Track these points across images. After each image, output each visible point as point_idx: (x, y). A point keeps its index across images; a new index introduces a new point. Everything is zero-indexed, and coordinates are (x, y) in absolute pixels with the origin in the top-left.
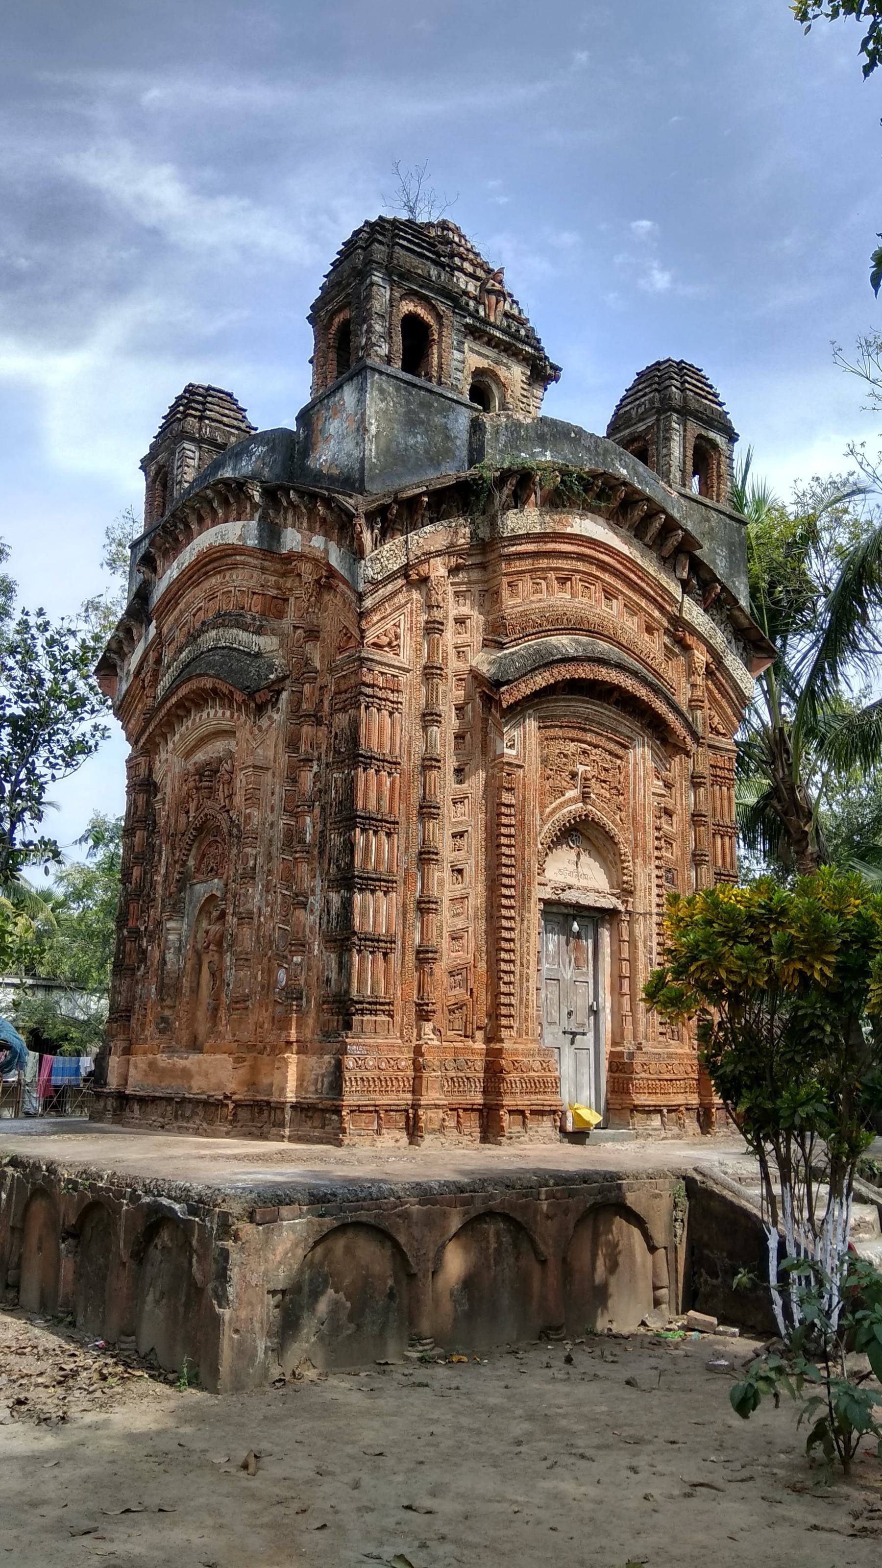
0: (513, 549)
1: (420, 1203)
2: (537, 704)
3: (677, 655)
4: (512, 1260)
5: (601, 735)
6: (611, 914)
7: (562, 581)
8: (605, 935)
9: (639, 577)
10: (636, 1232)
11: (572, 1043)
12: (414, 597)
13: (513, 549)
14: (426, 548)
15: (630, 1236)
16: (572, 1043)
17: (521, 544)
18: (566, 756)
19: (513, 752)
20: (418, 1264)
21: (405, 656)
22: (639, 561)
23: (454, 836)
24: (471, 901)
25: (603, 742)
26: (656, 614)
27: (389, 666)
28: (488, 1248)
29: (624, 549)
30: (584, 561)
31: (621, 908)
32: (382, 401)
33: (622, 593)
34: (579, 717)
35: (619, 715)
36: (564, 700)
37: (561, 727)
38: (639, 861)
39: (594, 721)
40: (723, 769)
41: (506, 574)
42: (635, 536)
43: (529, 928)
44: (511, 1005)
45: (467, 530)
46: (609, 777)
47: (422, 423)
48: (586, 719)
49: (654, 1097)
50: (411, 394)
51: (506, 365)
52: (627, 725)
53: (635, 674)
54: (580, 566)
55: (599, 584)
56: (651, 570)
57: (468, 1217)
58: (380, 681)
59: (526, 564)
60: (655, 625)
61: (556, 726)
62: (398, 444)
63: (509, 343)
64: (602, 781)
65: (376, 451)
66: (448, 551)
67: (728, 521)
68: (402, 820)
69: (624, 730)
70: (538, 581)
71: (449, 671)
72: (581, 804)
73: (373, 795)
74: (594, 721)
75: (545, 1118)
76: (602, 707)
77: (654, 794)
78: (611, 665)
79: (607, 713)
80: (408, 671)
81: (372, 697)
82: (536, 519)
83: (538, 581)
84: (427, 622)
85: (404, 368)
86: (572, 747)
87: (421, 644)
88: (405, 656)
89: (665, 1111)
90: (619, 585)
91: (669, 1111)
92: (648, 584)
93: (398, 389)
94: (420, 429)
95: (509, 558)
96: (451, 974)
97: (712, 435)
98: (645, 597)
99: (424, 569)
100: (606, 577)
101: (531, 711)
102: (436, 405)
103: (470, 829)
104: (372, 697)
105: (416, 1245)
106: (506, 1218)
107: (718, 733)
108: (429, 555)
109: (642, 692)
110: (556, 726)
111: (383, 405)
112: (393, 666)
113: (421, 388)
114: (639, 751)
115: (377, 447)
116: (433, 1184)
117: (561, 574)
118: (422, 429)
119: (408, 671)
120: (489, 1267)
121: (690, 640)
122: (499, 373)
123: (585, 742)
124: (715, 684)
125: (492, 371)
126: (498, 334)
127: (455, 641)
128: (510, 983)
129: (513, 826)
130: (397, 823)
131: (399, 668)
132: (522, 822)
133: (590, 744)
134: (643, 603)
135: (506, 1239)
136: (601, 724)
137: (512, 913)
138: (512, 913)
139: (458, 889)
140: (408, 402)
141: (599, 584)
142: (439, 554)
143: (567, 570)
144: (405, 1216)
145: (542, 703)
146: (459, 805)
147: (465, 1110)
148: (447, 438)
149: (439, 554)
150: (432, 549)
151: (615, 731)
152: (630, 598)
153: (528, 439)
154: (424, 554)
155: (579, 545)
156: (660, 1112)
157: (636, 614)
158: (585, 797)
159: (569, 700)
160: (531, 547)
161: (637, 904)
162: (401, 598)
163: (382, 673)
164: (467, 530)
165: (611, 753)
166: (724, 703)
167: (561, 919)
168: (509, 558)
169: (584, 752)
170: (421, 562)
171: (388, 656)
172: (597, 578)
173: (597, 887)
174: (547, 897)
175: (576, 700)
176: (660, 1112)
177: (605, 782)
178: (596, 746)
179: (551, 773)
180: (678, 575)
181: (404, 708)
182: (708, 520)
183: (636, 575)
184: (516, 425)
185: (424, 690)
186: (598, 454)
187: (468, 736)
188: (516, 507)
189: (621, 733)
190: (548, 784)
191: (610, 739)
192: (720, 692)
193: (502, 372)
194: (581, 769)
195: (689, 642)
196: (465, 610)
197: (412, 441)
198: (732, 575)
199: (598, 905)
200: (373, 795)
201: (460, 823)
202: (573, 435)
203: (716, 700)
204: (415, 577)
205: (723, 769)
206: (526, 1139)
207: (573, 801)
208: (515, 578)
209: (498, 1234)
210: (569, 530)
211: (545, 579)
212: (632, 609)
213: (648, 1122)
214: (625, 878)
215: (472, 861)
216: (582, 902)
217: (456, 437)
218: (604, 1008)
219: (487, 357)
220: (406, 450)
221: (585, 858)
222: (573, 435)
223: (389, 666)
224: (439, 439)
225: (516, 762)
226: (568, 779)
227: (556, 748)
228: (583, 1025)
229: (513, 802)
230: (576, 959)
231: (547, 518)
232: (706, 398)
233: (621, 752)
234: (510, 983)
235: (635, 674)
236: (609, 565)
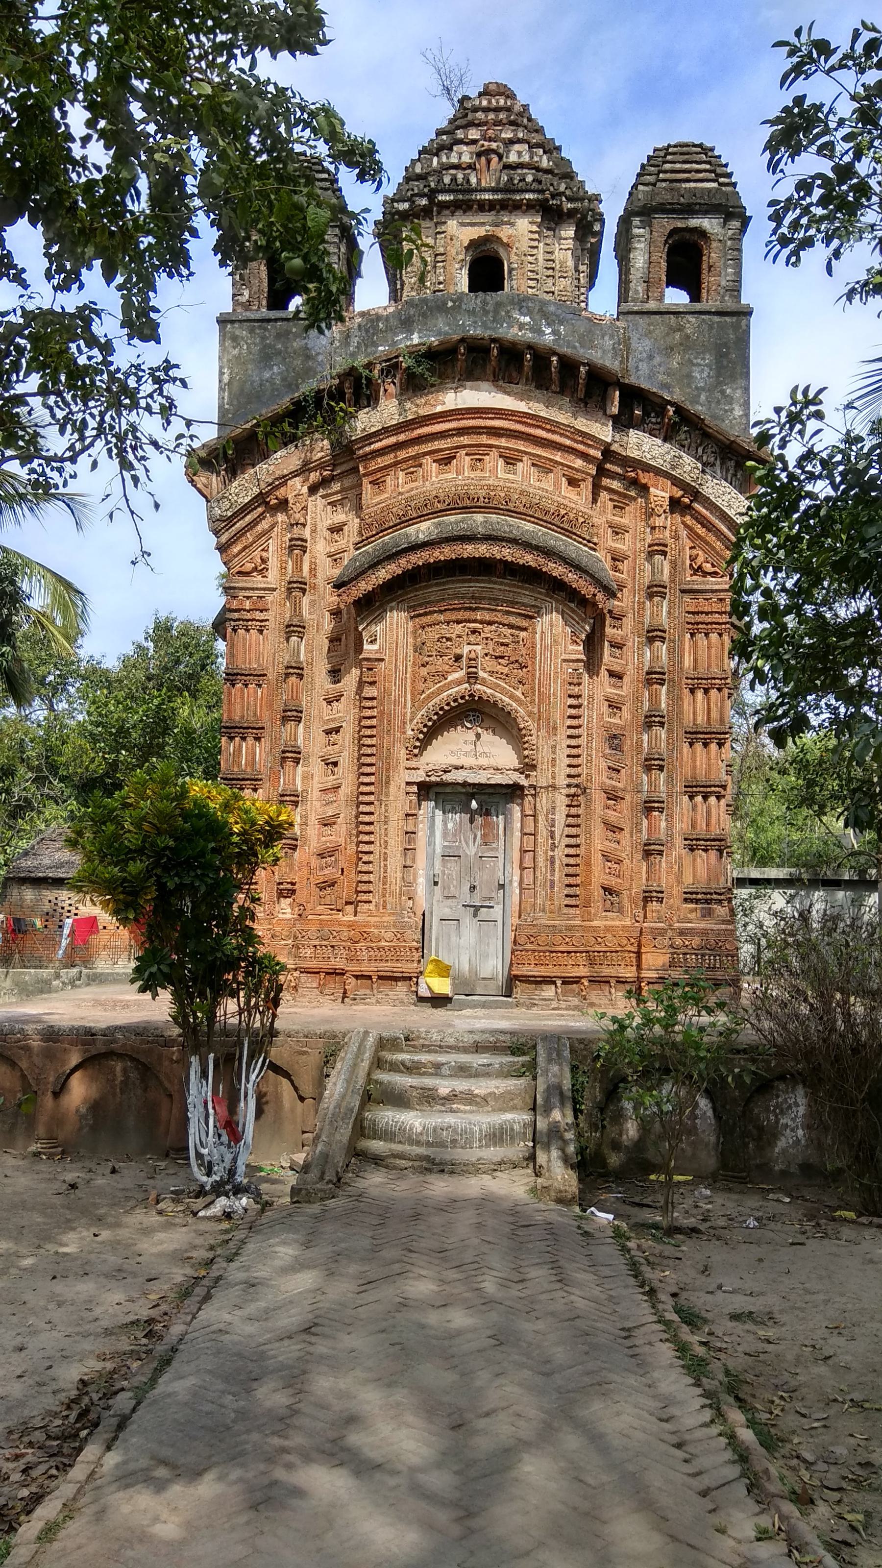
0: (367, 449)
1: (41, 1040)
2: (401, 596)
3: (635, 499)
4: (139, 1092)
5: (495, 610)
6: (513, 792)
7: (446, 461)
8: (516, 809)
9: (548, 431)
10: (285, 1082)
11: (475, 915)
12: (280, 519)
13: (367, 449)
14: (278, 473)
15: (277, 1085)
16: (475, 915)
17: (381, 440)
18: (448, 639)
19: (375, 647)
20: (37, 1085)
21: (273, 577)
22: (542, 414)
23: (328, 732)
24: (343, 791)
25: (499, 617)
26: (579, 463)
27: (253, 589)
28: (114, 1080)
29: (521, 406)
30: (468, 434)
31: (524, 782)
32: (234, 348)
33: (527, 453)
34: (463, 598)
35: (514, 586)
36: (437, 585)
37: (441, 612)
38: (543, 733)
39: (484, 598)
40: (712, 613)
41: (365, 475)
42: (537, 387)
43: (386, 811)
44: (370, 882)
45: (326, 442)
46: (507, 651)
47: (279, 353)
48: (473, 597)
49: (542, 968)
50: (266, 329)
51: (507, 223)
52: (526, 595)
53: (514, 541)
54: (465, 440)
55: (494, 453)
56: (562, 417)
57: (88, 1055)
58: (247, 605)
59: (388, 459)
60: (578, 476)
61: (435, 612)
62: (253, 382)
63: (503, 200)
64: (496, 658)
65: (229, 397)
66: (304, 469)
67: (716, 319)
68: (267, 725)
69: (526, 600)
70: (412, 469)
71: (320, 580)
72: (467, 685)
73: (238, 707)
74: (484, 598)
75: (399, 984)
76: (490, 582)
77: (565, 660)
78: (478, 539)
79: (498, 587)
80: (274, 590)
81: (239, 620)
82: (394, 410)
83: (412, 469)
84: (291, 540)
85: (270, 307)
86: (458, 629)
87: (286, 562)
88: (273, 577)
89: (559, 982)
90: (520, 445)
91: (564, 983)
92: (562, 435)
93: (252, 331)
94: (277, 359)
95: (366, 458)
96: (321, 856)
97: (694, 222)
98: (559, 449)
99: (281, 493)
100: (503, 442)
101: (394, 604)
102: (294, 330)
103: (344, 724)
104: (239, 620)
105: (37, 1071)
106: (132, 1059)
107: (705, 574)
108: (284, 480)
109: (529, 559)
110: (435, 612)
111: (236, 352)
112: (257, 589)
113: (276, 320)
114: (546, 619)
115: (230, 393)
116: (30, 1028)
117: (439, 456)
118: (280, 358)
119: (274, 590)
120: (114, 1095)
121: (644, 478)
122: (501, 235)
123: (475, 621)
124: (696, 519)
125: (493, 236)
126: (487, 196)
127: (328, 550)
128: (370, 862)
129: (375, 717)
130: (263, 728)
131: (264, 589)
132: (382, 713)
133: (481, 622)
134: (558, 457)
135: (133, 1075)
136: (495, 599)
137: (371, 798)
138: (371, 798)
139: (330, 781)
140: (263, 338)
141: (494, 453)
142: (295, 474)
143: (446, 449)
144: (27, 1049)
145: (407, 593)
146: (335, 704)
147: (327, 973)
148: (308, 357)
149: (295, 474)
150: (285, 472)
151: (512, 603)
152: (538, 456)
153: (389, 329)
154: (276, 479)
155: (459, 420)
156: (554, 983)
157: (551, 471)
158: (472, 677)
159: (444, 584)
160: (392, 440)
161: (539, 777)
162: (265, 525)
163: (248, 598)
164: (326, 442)
165: (511, 626)
166: (711, 538)
167: (463, 797)
168: (366, 458)
169: (474, 632)
170: (277, 487)
171: (257, 580)
172: (491, 446)
173: (495, 764)
174: (419, 779)
175: (453, 582)
176: (554, 983)
177: (502, 657)
178: (490, 623)
179: (428, 659)
180: (608, 412)
181: (271, 624)
182: (680, 329)
183: (543, 429)
184: (372, 321)
185: (288, 604)
186: (486, 312)
187: (344, 637)
188: (369, 406)
189: (523, 604)
190: (424, 671)
191: (508, 613)
192: (703, 526)
193: (504, 233)
194: (466, 649)
195: (644, 481)
196: (340, 517)
197: (267, 375)
198: (720, 383)
199: (492, 782)
200: (238, 707)
201: (333, 720)
202: (450, 304)
203: (699, 536)
204: (274, 502)
205: (712, 613)
206: (373, 1000)
207: (459, 683)
208: (379, 475)
209: (125, 1070)
210: (439, 409)
211: (420, 465)
212: (544, 467)
213: (537, 992)
214: (526, 753)
215: (346, 753)
216: (470, 781)
217: (318, 354)
218: (511, 881)
219: (483, 224)
220: (261, 385)
221: (487, 736)
222: (450, 304)
223: (253, 589)
224: (298, 362)
225: (378, 656)
226: (451, 662)
227: (432, 634)
228: (490, 899)
229: (375, 694)
230: (484, 836)
231: (408, 405)
232: (688, 180)
233: (524, 623)
234: (370, 862)
235: (514, 541)
236: (503, 429)
